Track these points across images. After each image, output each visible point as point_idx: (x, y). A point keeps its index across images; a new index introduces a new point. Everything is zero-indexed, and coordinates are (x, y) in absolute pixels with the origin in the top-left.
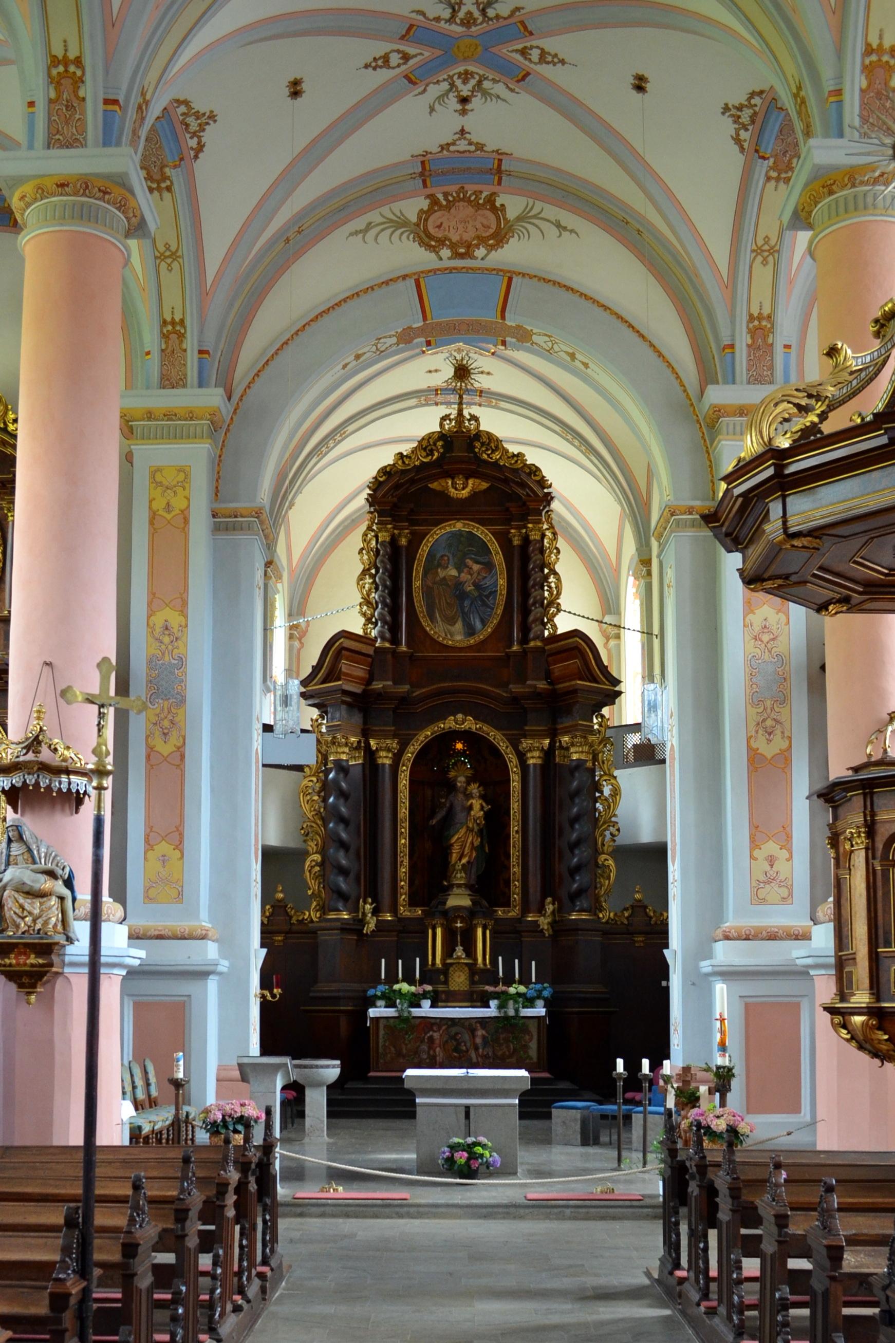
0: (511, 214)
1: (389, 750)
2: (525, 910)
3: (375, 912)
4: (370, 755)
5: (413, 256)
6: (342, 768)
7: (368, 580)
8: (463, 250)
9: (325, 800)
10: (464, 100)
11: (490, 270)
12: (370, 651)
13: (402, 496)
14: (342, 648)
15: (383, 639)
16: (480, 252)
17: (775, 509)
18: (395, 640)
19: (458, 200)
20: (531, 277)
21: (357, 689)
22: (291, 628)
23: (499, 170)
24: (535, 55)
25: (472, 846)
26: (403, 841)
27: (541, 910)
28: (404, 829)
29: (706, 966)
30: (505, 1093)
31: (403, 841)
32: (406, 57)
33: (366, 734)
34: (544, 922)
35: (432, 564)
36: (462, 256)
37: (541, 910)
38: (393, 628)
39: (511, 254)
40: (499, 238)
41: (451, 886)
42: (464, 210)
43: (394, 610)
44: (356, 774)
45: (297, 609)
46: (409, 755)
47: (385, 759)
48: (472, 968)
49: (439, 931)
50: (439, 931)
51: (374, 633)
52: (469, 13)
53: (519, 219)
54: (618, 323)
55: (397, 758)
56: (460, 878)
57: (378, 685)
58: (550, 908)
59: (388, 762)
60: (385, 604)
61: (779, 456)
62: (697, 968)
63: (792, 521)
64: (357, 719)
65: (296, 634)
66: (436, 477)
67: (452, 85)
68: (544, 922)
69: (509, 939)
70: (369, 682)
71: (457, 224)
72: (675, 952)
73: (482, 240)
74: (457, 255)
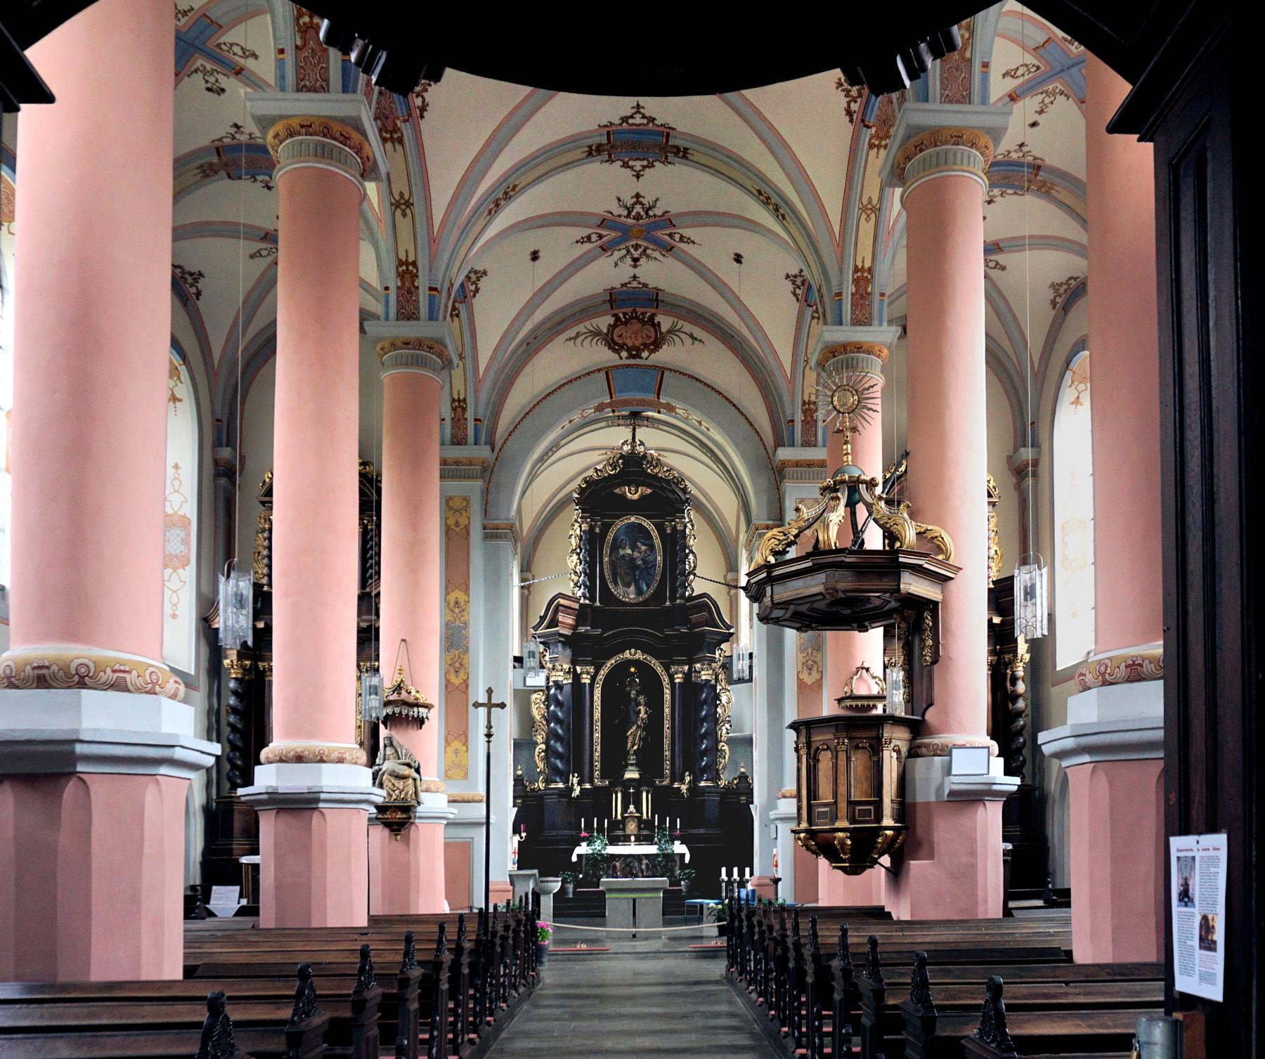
0: (664, 328)
1: (588, 673)
2: (672, 782)
3: (579, 784)
4: (577, 677)
5: (603, 355)
6: (559, 686)
7: (575, 557)
8: (635, 353)
9: (548, 707)
10: (636, 260)
11: (650, 367)
12: (576, 606)
13: (597, 498)
14: (559, 605)
15: (585, 598)
16: (645, 354)
17: (768, 589)
18: (592, 599)
19: (631, 318)
20: (675, 371)
21: (567, 632)
22: (522, 587)
23: (657, 300)
24: (677, 237)
25: (640, 739)
26: (597, 735)
27: (682, 781)
28: (598, 726)
29: (772, 815)
30: (656, 890)
31: (597, 735)
32: (601, 237)
33: (574, 662)
34: (684, 788)
35: (616, 546)
36: (634, 357)
37: (682, 781)
38: (591, 589)
39: (664, 356)
40: (656, 345)
41: (627, 765)
42: (636, 325)
43: (591, 576)
44: (567, 689)
45: (526, 569)
46: (603, 672)
47: (586, 680)
48: (640, 818)
49: (619, 795)
50: (619, 795)
51: (579, 593)
52: (638, 213)
53: (670, 332)
54: (730, 406)
55: (593, 679)
56: (632, 759)
57: (582, 629)
58: (688, 779)
59: (588, 681)
60: (586, 574)
61: (768, 567)
62: (768, 816)
63: (776, 597)
64: (568, 652)
65: (526, 590)
66: (618, 485)
67: (628, 251)
68: (684, 788)
69: (665, 802)
70: (575, 627)
71: (630, 335)
72: (756, 810)
73: (646, 346)
74: (631, 356)
